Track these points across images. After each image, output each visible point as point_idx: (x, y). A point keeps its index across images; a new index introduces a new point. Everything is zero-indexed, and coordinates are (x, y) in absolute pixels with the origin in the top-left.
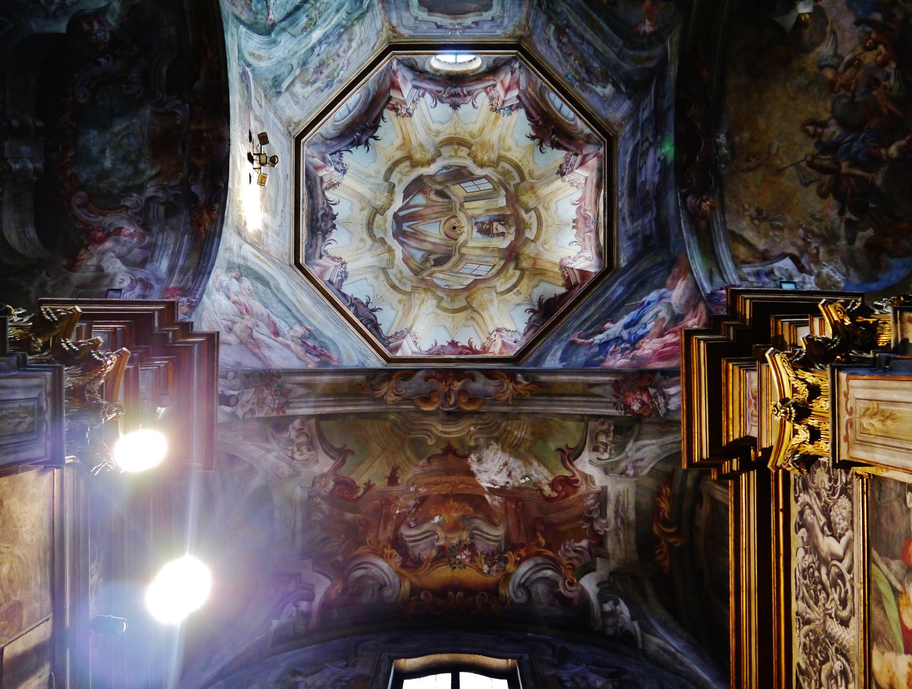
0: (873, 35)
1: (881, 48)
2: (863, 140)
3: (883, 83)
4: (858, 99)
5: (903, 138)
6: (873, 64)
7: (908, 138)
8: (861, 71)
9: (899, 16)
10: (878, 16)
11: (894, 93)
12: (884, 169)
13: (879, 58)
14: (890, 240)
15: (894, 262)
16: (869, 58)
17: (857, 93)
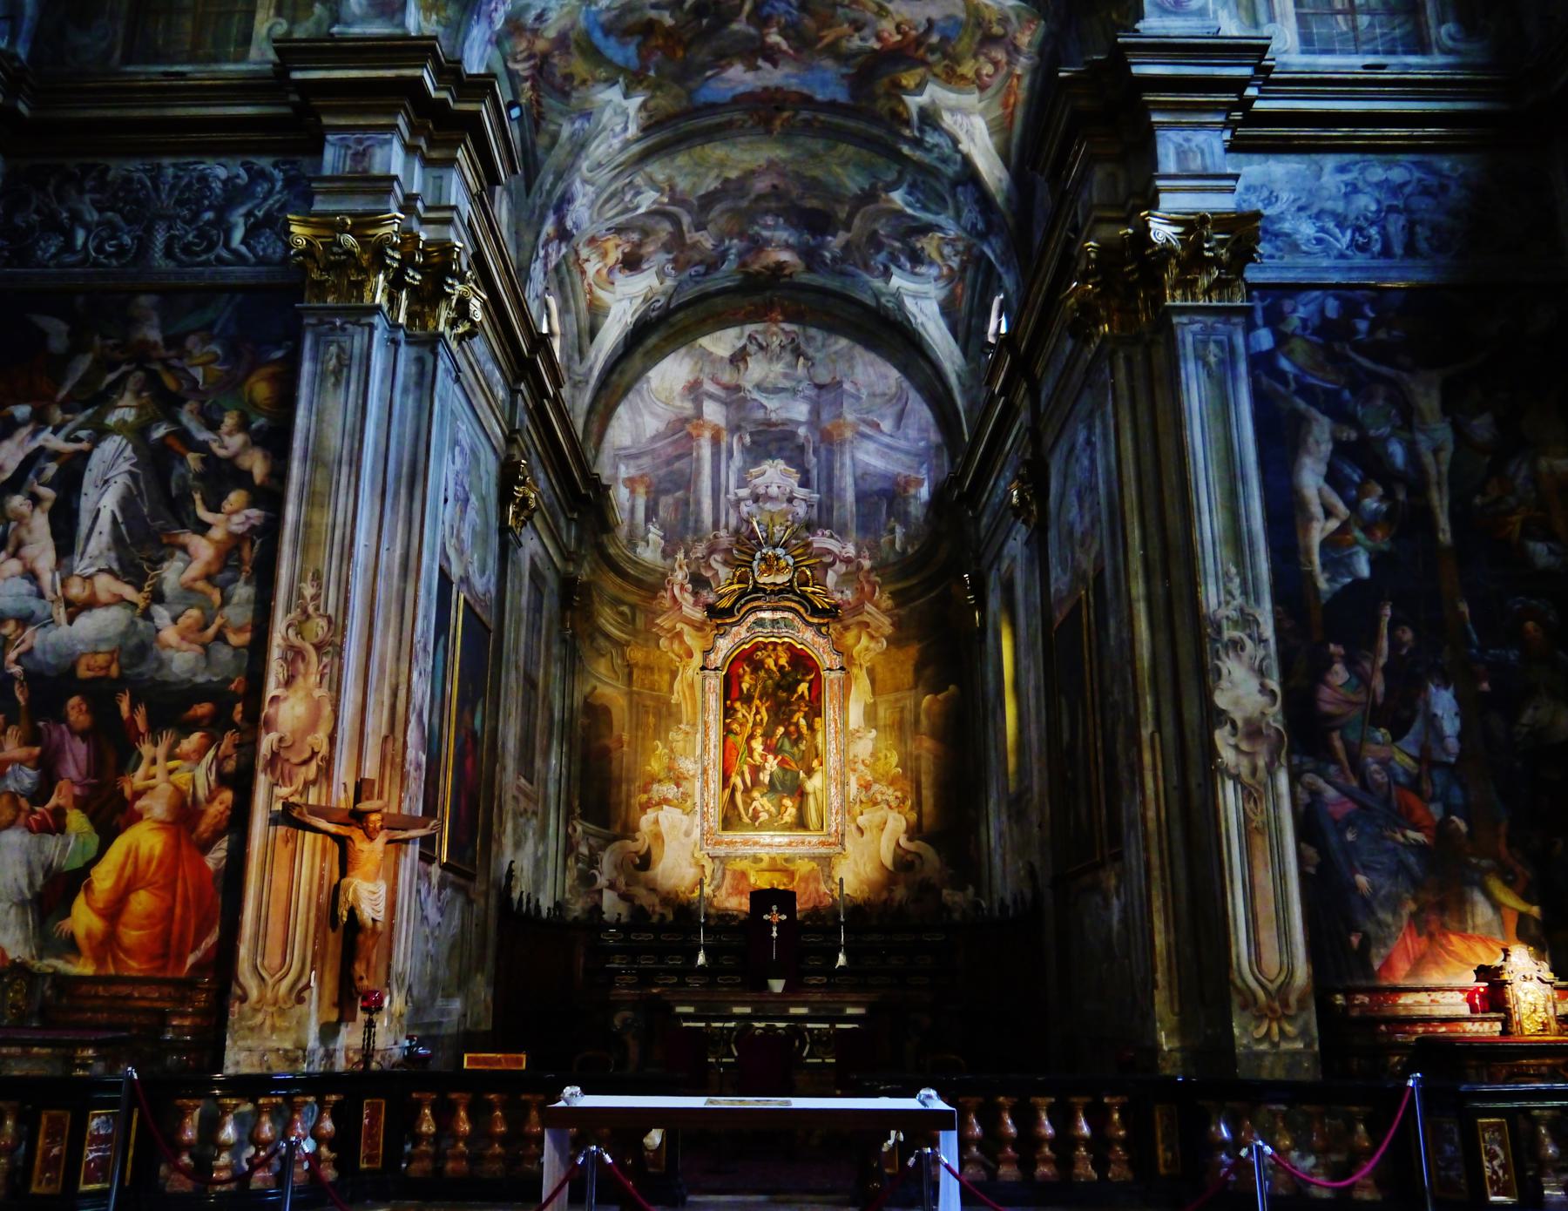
0: (913, 33)
1: (899, 38)
2: (790, 13)
3: (857, 35)
4: (840, 11)
5: (790, 46)
6: (879, 28)
7: (791, 52)
8: (874, 18)
9: (931, 58)
10: (934, 39)
11: (844, 43)
12: (752, 31)
13: (886, 35)
14: (660, 41)
15: (632, 50)
16: (887, 26)
17: (847, 10)
